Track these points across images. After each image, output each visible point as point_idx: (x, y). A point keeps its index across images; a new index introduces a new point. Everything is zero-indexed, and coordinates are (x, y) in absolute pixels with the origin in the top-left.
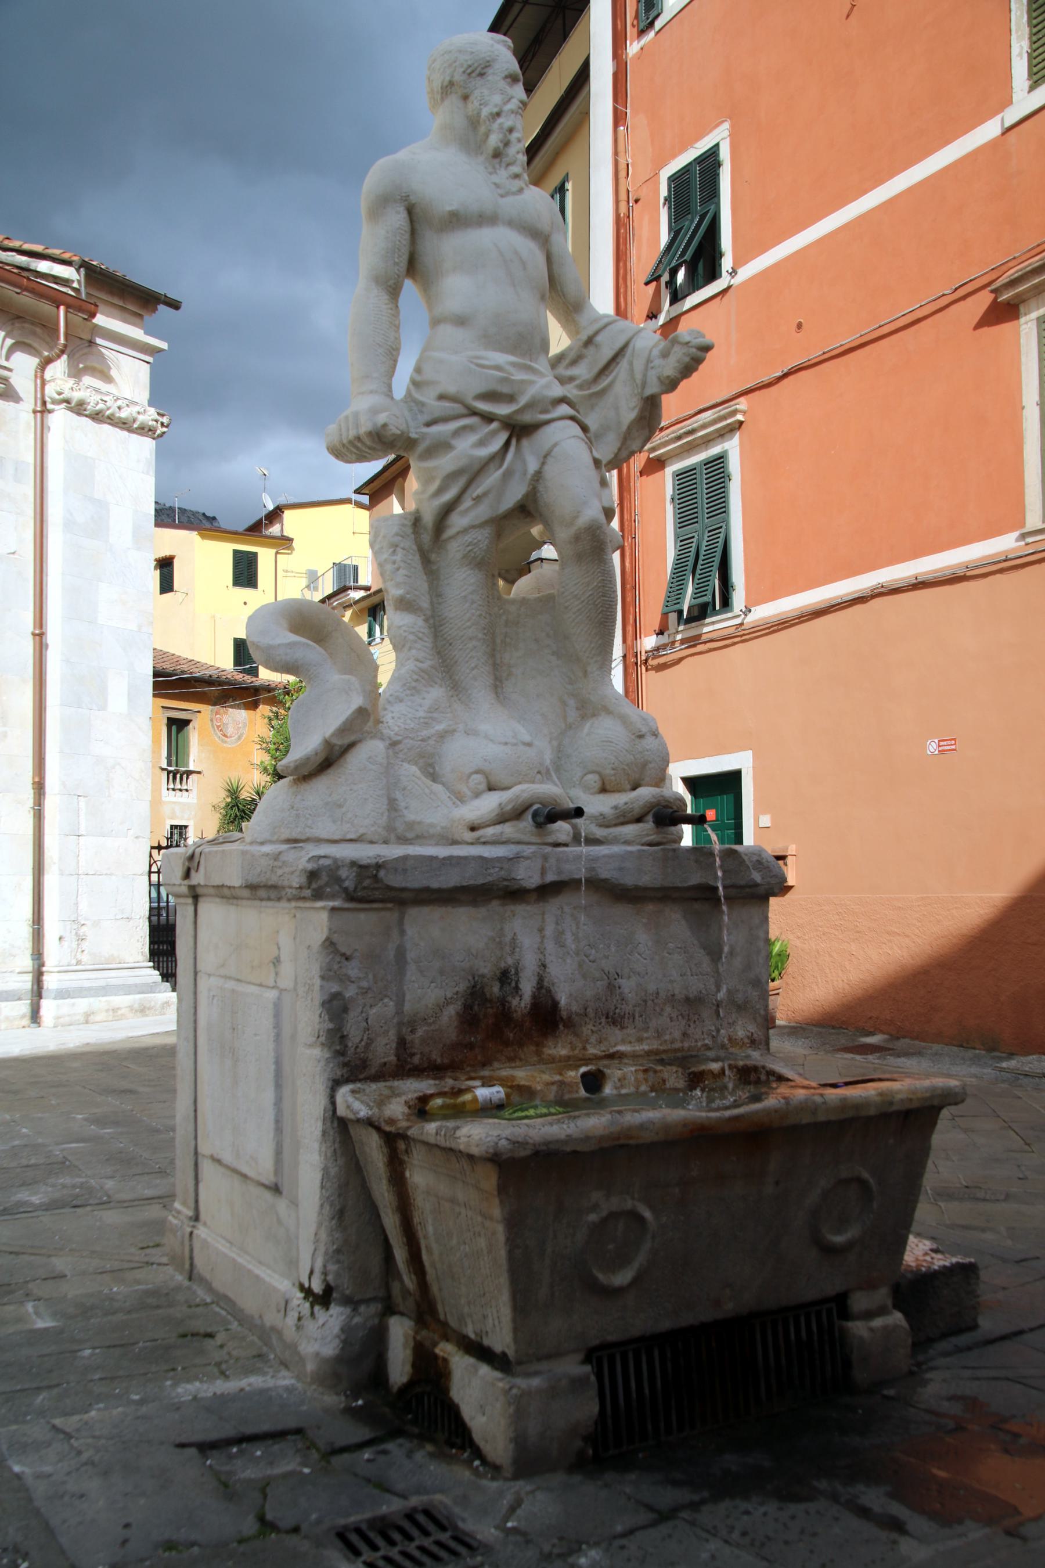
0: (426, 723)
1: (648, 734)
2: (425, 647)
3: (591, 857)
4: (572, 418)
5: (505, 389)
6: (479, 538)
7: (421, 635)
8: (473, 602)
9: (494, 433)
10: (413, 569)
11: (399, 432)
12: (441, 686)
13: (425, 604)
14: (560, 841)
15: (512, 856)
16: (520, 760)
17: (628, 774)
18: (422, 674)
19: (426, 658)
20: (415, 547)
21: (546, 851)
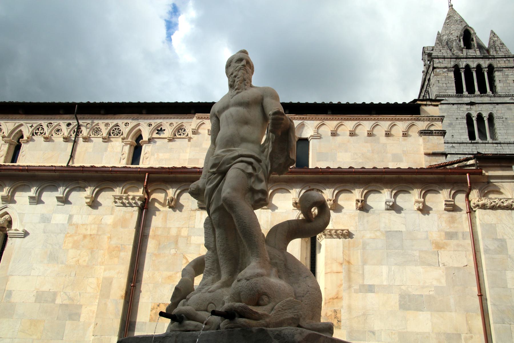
0: (200, 290)
1: (243, 279)
2: (209, 262)
3: (195, 336)
4: (242, 161)
5: (217, 162)
6: (215, 217)
7: (208, 258)
8: (218, 241)
9: (215, 178)
10: (209, 235)
11: (194, 189)
12: (214, 276)
13: (212, 246)
14: (188, 329)
15: (164, 336)
16: (200, 298)
17: (234, 299)
18: (207, 272)
19: (209, 266)
20: (210, 226)
21: (178, 333)
